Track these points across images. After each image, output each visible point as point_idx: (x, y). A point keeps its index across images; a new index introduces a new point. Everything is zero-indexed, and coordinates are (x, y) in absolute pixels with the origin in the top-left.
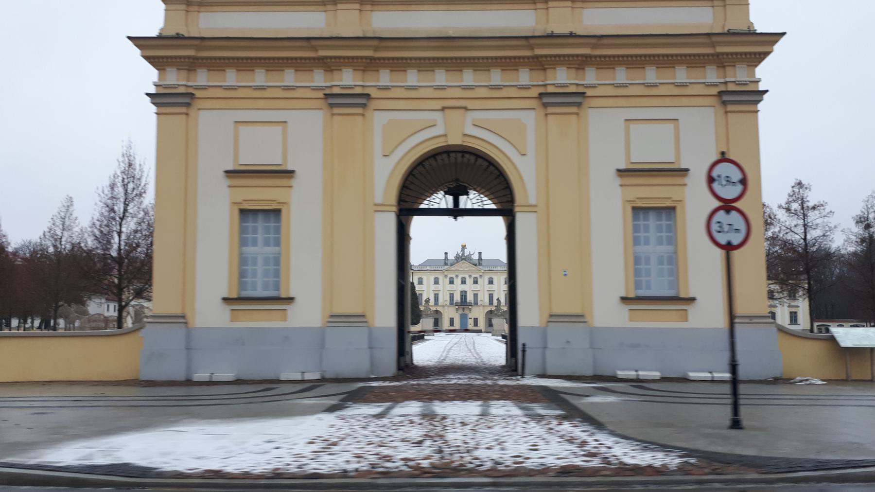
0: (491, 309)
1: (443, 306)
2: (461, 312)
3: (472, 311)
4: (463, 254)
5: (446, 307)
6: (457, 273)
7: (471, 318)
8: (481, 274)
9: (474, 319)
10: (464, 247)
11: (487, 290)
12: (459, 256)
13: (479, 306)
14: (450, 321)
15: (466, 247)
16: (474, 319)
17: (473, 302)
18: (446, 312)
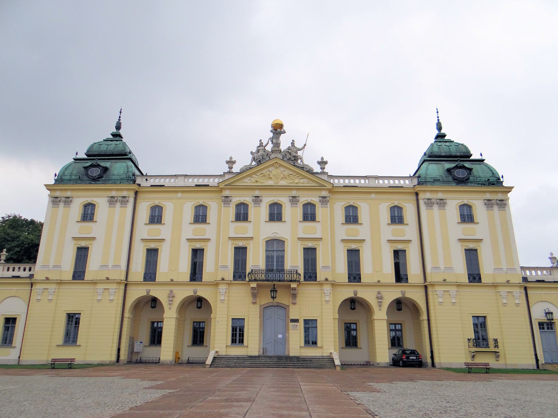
0: (356, 293)
1: (216, 284)
2: (266, 299)
3: (298, 300)
4: (277, 145)
5: (222, 288)
6: (257, 193)
7: (296, 321)
8: (324, 193)
9: (306, 322)
10: (278, 129)
11: (343, 241)
12: (264, 150)
13: (321, 284)
14: (234, 329)
15: (285, 128)
16: (306, 322)
17: (301, 271)
18: (222, 301)
